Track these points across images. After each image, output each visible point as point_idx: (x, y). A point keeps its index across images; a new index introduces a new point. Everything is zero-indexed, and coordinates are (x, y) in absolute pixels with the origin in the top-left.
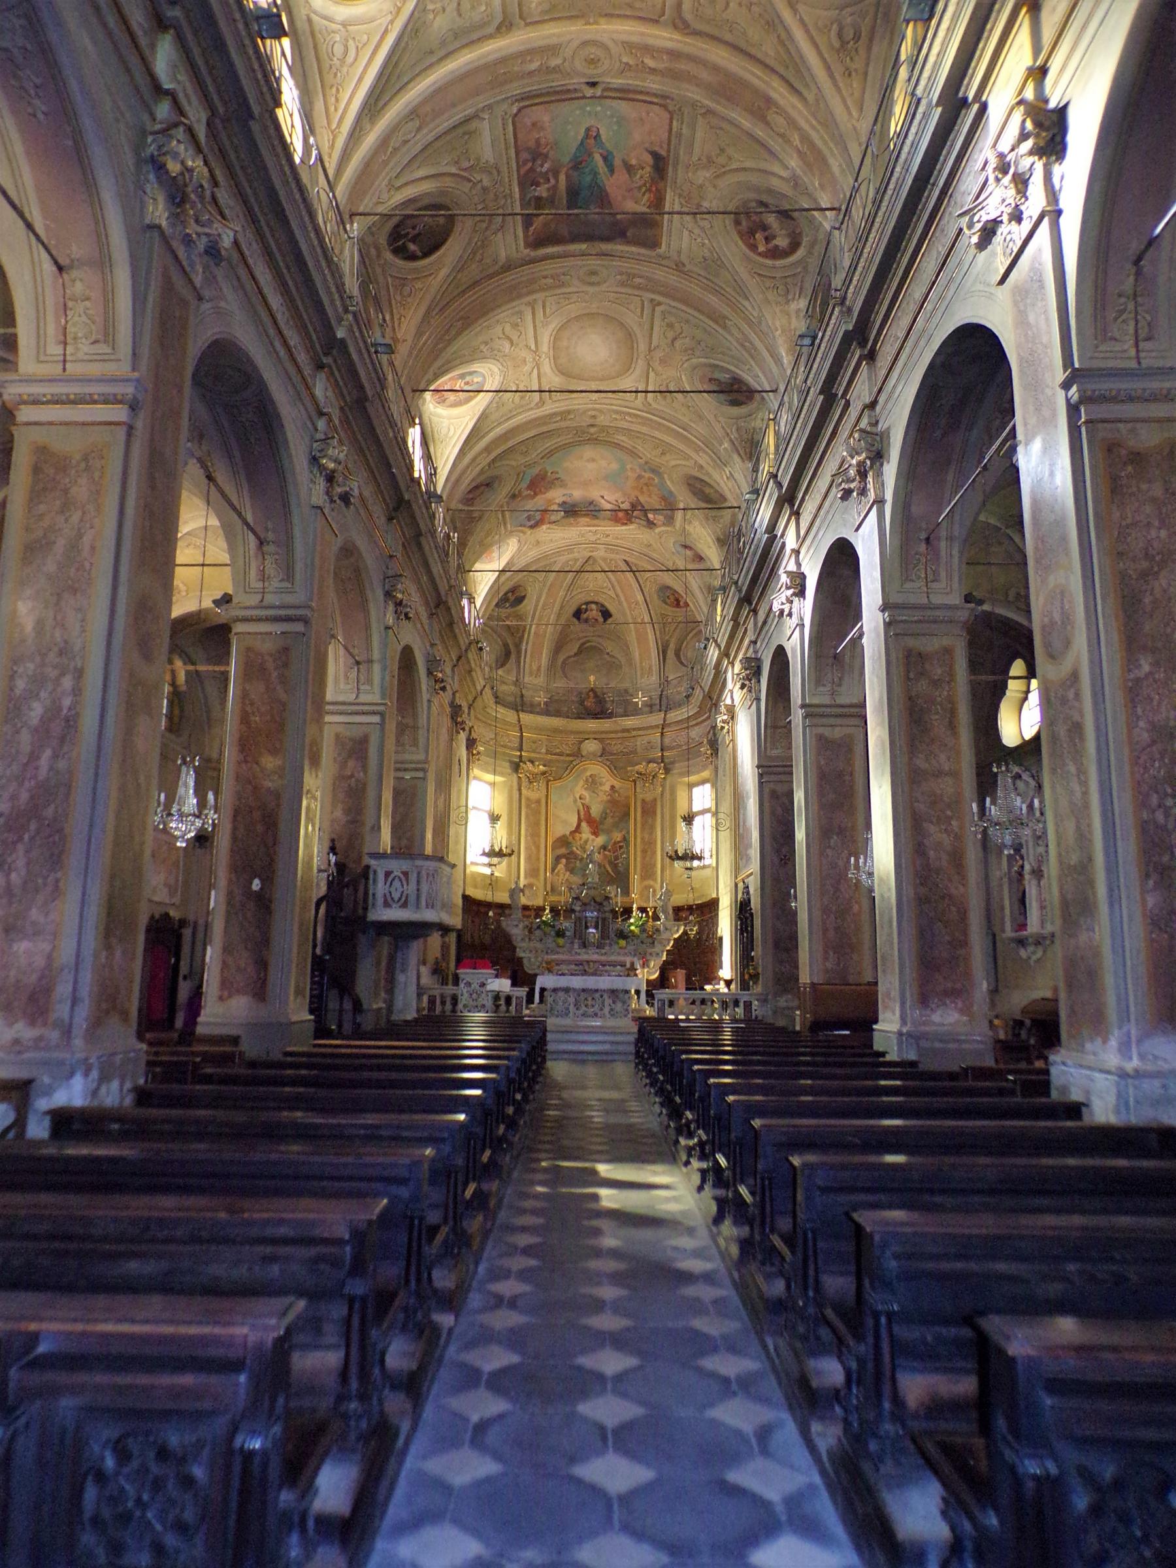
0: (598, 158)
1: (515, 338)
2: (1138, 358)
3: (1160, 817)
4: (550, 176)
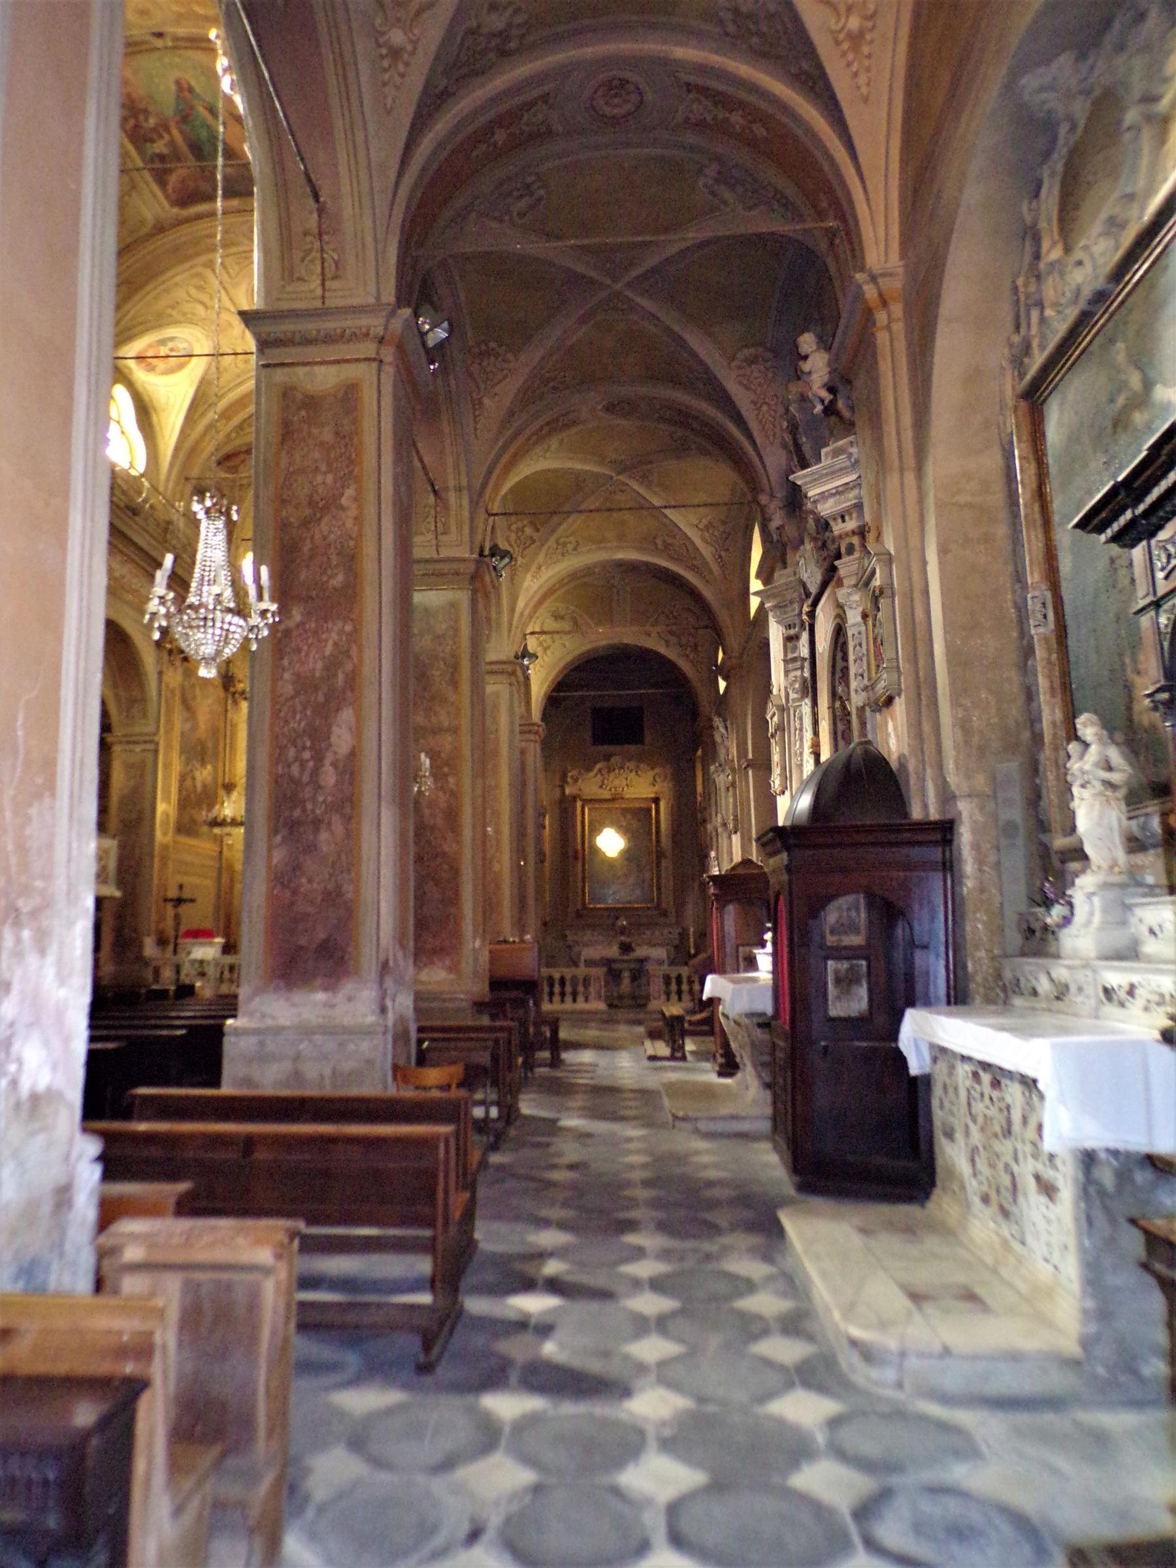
0: (202, 111)
1: (206, 300)
2: (323, 297)
3: (295, 770)
4: (161, 130)
